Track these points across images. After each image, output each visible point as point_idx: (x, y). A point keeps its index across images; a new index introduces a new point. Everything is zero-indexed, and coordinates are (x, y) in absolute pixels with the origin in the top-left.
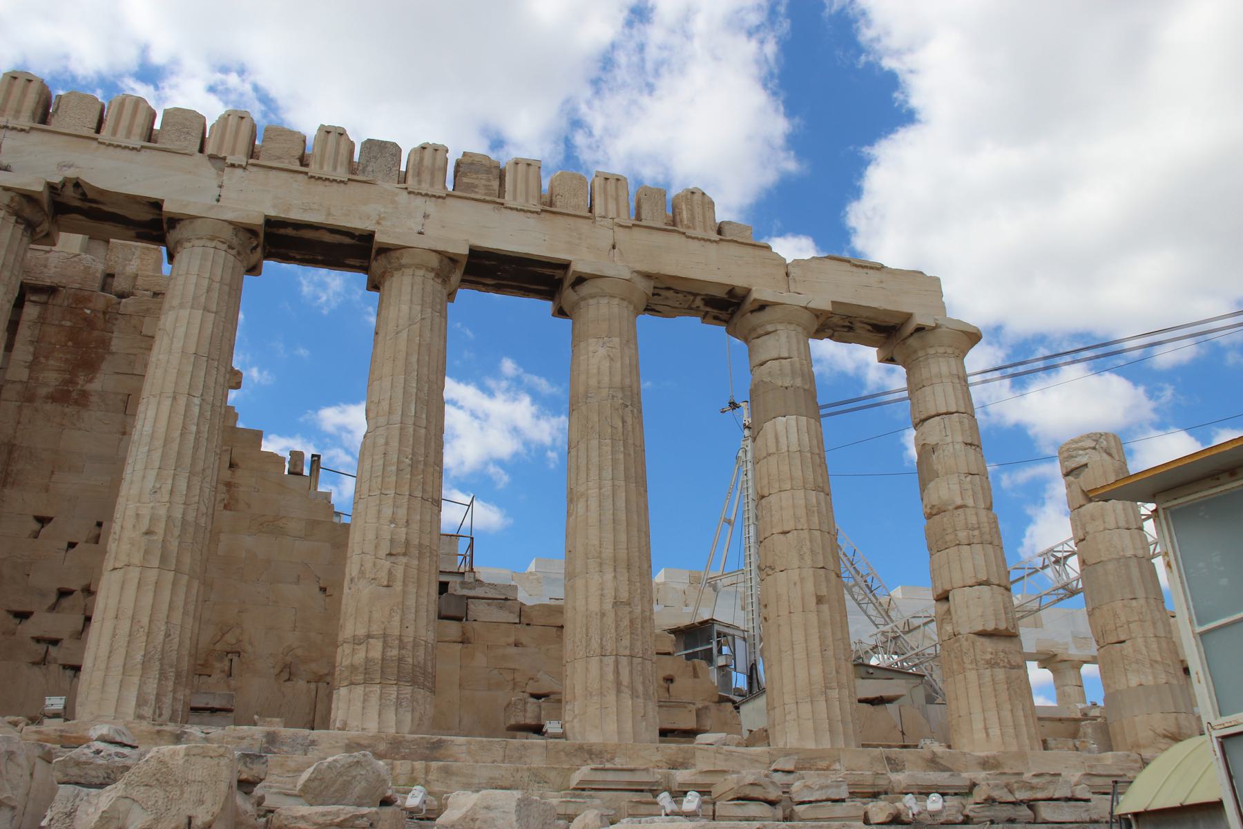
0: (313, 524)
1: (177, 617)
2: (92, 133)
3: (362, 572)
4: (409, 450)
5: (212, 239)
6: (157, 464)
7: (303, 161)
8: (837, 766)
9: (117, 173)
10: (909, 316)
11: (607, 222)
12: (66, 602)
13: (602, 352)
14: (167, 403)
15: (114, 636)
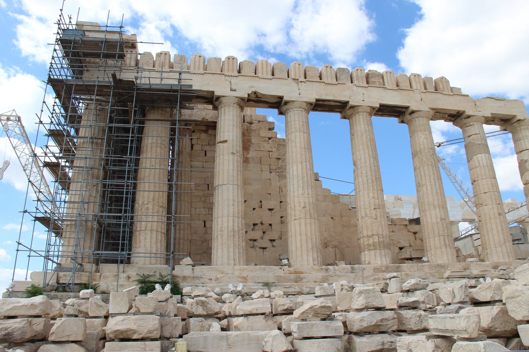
0: (325, 196)
1: (317, 232)
2: (254, 74)
3: (366, 215)
4: (374, 174)
5: (300, 108)
6: (302, 185)
7: (320, 78)
8: (511, 267)
9: (269, 89)
10: (515, 116)
11: (418, 91)
12: (256, 227)
13: (423, 136)
14: (300, 165)
15: (301, 240)
